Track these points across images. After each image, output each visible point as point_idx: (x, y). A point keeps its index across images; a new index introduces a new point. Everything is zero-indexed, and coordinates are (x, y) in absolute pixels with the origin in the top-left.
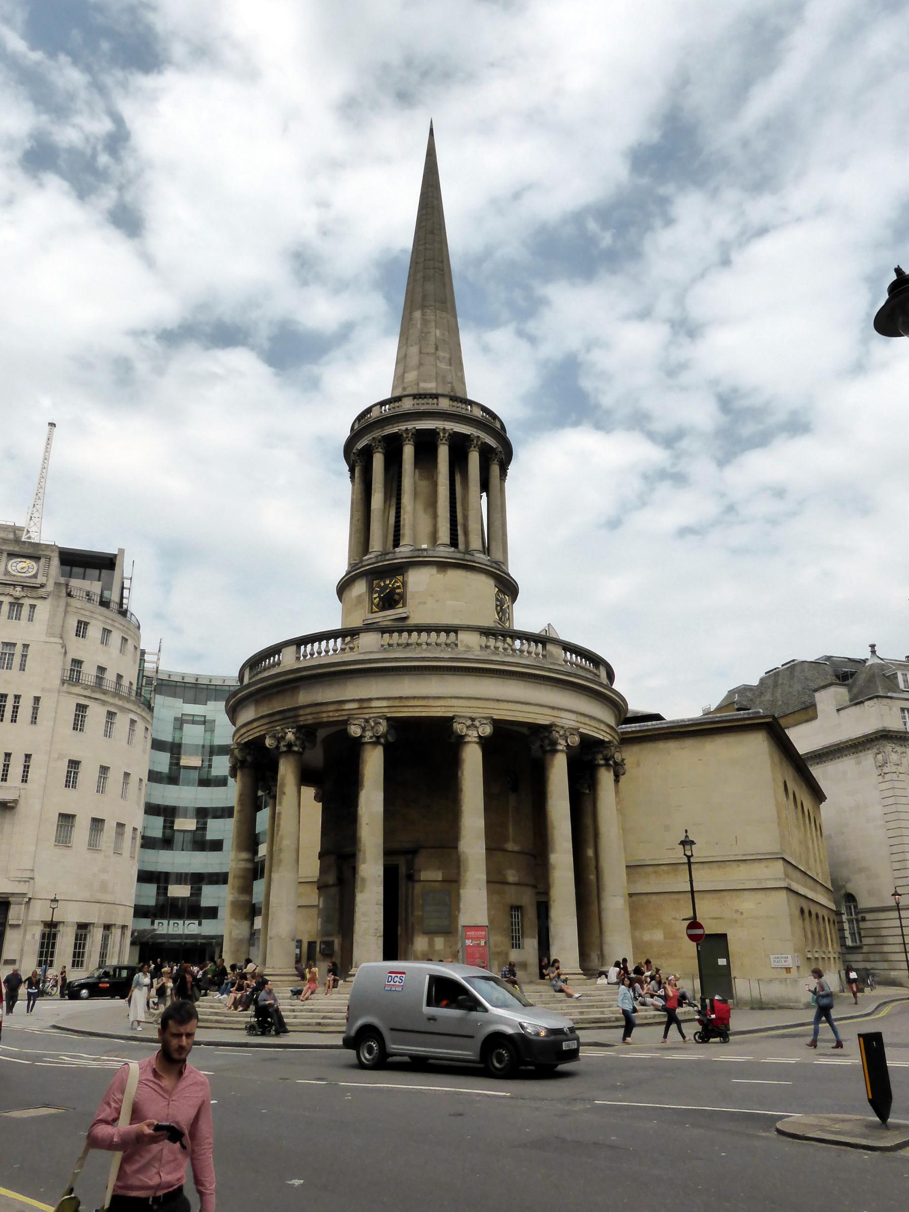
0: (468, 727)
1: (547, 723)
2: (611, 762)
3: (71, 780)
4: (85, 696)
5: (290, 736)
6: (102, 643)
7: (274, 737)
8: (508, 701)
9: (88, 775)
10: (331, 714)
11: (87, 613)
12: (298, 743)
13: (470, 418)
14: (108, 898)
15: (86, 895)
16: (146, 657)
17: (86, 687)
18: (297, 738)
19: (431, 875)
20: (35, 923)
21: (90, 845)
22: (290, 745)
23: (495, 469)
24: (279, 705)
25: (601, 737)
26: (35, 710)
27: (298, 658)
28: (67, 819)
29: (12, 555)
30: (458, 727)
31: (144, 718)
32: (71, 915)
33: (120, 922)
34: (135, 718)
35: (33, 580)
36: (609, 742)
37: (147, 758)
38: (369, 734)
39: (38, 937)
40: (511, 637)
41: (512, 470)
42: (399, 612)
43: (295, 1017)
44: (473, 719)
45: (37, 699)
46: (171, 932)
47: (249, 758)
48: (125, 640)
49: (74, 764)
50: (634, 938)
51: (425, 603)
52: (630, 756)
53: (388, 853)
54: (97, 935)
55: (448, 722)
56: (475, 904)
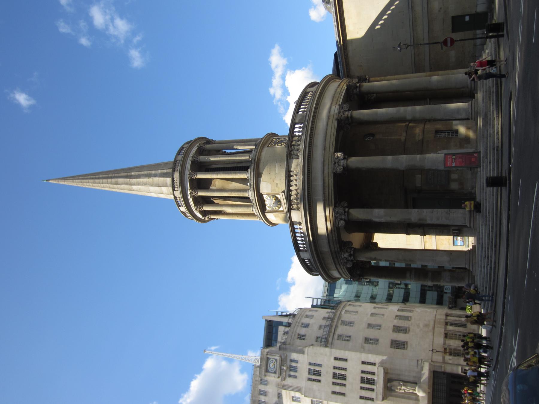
0: (339, 165)
1: (336, 122)
2: (358, 85)
4: (333, 336)
5: (346, 255)
6: (308, 327)
7: (346, 263)
8: (325, 144)
9: (372, 334)
10: (334, 235)
11: (293, 335)
12: (349, 251)
13: (183, 161)
14: (432, 323)
15: (431, 334)
16: (315, 304)
18: (347, 252)
19: (418, 181)
20: (444, 358)
21: (406, 333)
22: (350, 255)
23: (208, 146)
24: (330, 261)
25: (345, 91)
26: (340, 359)
27: (306, 251)
29: (267, 371)
30: (340, 169)
31: (344, 307)
32: (440, 340)
33: (444, 317)
34: (340, 322)
35: (278, 361)
36: (347, 86)
37: (363, 305)
38: (343, 217)
39: (450, 357)
40: (292, 142)
41: (210, 138)
43: (491, 257)
44: (335, 163)
46: (450, 291)
47: (358, 272)
48: (307, 316)
50: (454, 68)
51: (277, 184)
52: (356, 71)
53: (407, 207)
55: (337, 176)
56: (434, 159)
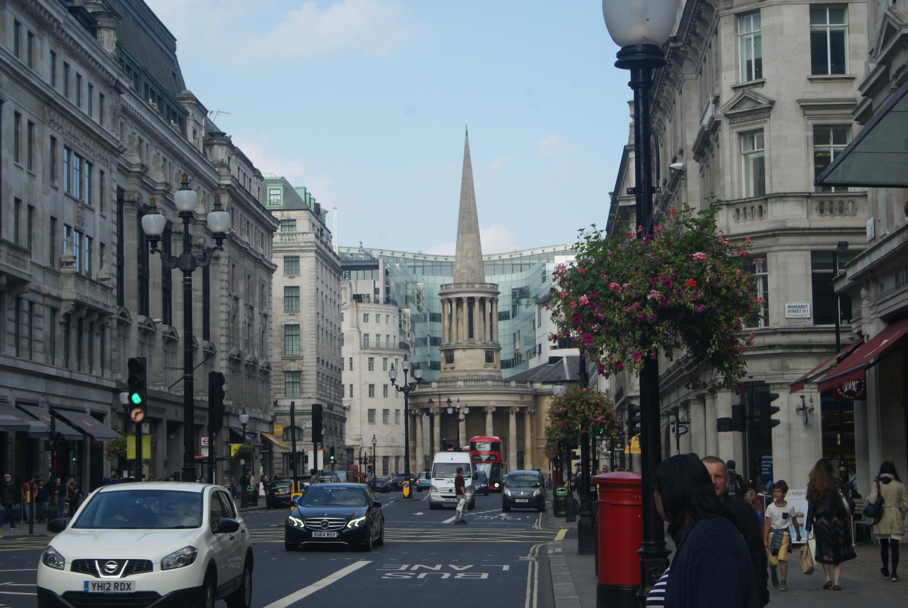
3: (371, 393)
15: (386, 444)
17: (372, 349)
26: (351, 364)
28: (372, 412)
42: (450, 365)
45: (351, 359)
48: (388, 316)
49: (372, 386)
54: (392, 461)
